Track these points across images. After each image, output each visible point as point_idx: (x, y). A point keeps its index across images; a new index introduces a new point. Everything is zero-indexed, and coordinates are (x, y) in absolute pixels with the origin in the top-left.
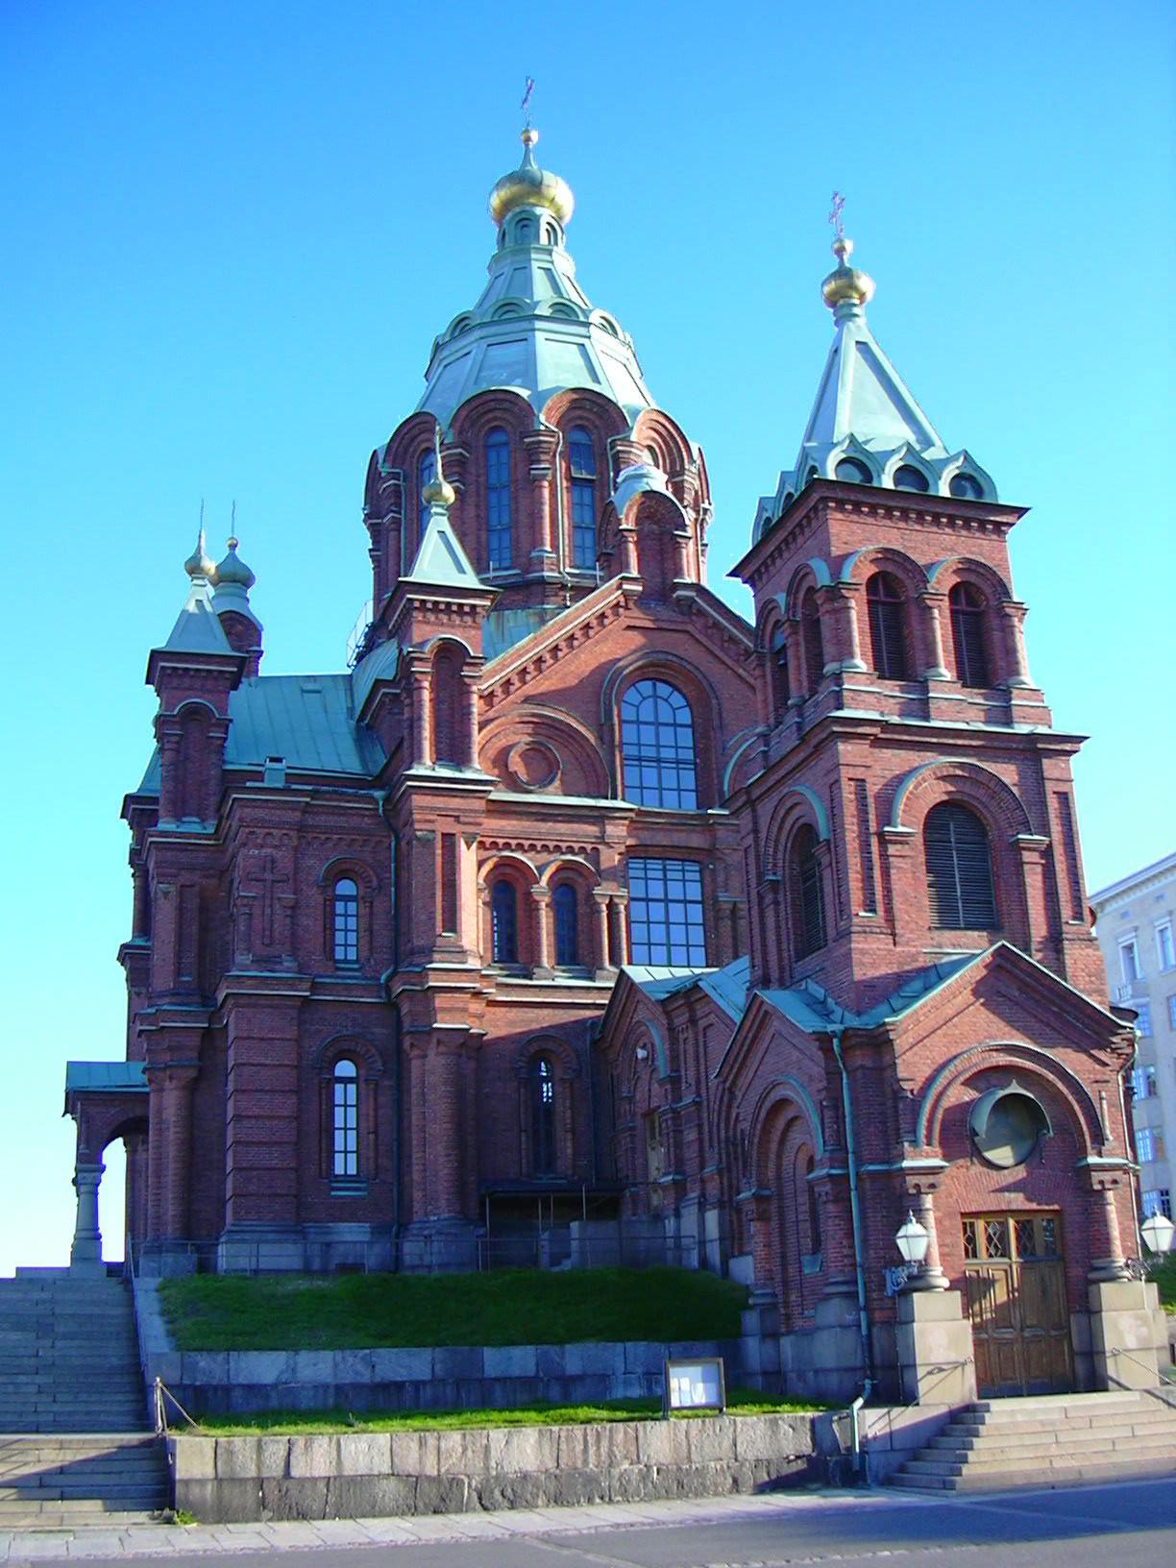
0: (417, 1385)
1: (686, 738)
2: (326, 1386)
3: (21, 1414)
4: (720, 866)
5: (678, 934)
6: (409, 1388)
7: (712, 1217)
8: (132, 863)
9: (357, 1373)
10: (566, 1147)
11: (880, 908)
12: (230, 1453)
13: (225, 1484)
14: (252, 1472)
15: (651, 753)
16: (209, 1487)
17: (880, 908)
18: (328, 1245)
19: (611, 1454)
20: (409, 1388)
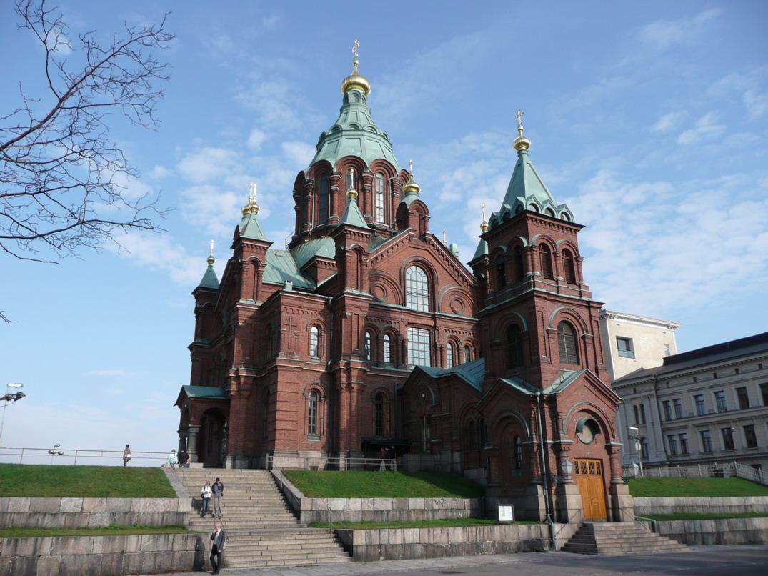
0: (387, 511)
1: (425, 287)
2: (359, 511)
3: (257, 521)
4: (436, 332)
5: (416, 354)
6: (385, 513)
7: (457, 456)
8: (196, 312)
9: (369, 506)
10: (387, 428)
11: (548, 354)
12: (370, 535)
13: (369, 547)
14: (377, 543)
15: (414, 291)
16: (364, 548)
17: (548, 354)
18: (307, 459)
19: (483, 536)
20: (385, 513)
